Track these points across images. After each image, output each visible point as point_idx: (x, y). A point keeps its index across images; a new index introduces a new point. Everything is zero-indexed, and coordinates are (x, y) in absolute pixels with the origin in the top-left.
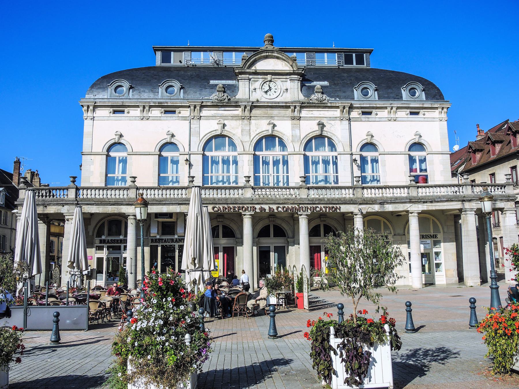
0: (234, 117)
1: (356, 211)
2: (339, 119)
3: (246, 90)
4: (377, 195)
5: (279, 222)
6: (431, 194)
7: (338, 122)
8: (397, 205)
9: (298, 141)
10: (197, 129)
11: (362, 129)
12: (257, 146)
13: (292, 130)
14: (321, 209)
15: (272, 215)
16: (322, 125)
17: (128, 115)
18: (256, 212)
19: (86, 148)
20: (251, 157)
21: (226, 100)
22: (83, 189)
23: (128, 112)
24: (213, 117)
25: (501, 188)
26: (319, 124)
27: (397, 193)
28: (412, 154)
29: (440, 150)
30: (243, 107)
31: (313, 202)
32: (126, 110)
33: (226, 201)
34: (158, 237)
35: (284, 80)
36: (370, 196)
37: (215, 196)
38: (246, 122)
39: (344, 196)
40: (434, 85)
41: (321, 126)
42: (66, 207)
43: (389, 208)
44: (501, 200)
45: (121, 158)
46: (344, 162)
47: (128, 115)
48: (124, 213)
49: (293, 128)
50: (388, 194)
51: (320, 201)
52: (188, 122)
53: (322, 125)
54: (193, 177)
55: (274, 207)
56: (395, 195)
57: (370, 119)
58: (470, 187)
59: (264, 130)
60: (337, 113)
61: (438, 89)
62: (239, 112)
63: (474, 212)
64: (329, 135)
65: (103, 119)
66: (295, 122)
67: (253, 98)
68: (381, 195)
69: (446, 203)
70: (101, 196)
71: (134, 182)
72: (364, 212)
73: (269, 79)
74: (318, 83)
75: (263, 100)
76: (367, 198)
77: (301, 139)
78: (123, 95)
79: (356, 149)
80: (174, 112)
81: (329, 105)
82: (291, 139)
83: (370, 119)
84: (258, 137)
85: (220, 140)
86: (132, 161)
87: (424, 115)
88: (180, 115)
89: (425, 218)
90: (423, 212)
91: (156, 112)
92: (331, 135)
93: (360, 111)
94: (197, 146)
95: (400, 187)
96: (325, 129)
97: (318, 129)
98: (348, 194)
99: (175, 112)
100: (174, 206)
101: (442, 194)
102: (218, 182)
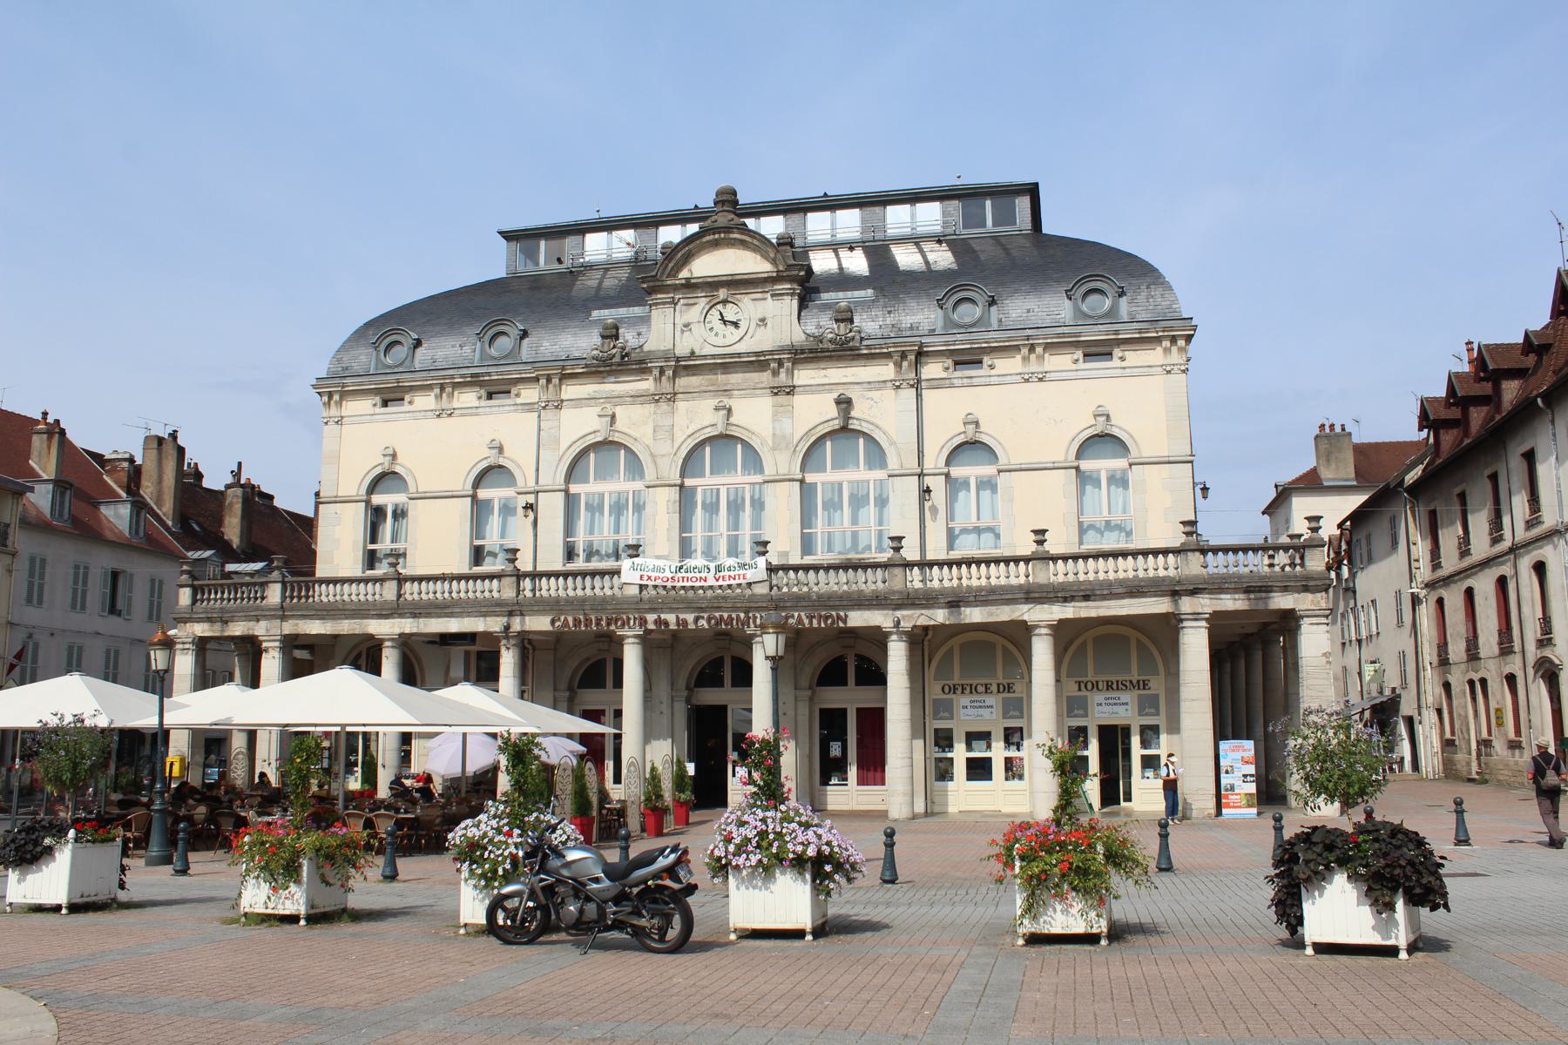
0: (637, 397)
3: (667, 328)
4: (946, 584)
6: (1091, 576)
8: (993, 609)
9: (787, 447)
11: (951, 406)
12: (691, 462)
13: (774, 421)
14: (800, 620)
16: (844, 403)
18: (648, 632)
21: (617, 359)
23: (411, 403)
26: (838, 402)
27: (998, 576)
28: (1086, 465)
29: (1163, 451)
30: (656, 372)
37: (561, 593)
38: (664, 406)
42: (263, 623)
43: (974, 615)
44: (1285, 589)
49: (775, 414)
51: (799, 601)
53: (844, 403)
55: (690, 617)
56: (993, 581)
60: (887, 371)
62: (647, 385)
64: (865, 428)
66: (782, 399)
67: (682, 350)
68: (955, 582)
69: (1126, 601)
70: (331, 598)
72: (906, 625)
74: (841, 295)
79: (935, 459)
84: (691, 443)
85: (605, 454)
86: (417, 510)
87: (1122, 359)
88: (519, 401)
91: (468, 398)
94: (553, 475)
96: (853, 414)
101: (1121, 575)
102: (591, 554)
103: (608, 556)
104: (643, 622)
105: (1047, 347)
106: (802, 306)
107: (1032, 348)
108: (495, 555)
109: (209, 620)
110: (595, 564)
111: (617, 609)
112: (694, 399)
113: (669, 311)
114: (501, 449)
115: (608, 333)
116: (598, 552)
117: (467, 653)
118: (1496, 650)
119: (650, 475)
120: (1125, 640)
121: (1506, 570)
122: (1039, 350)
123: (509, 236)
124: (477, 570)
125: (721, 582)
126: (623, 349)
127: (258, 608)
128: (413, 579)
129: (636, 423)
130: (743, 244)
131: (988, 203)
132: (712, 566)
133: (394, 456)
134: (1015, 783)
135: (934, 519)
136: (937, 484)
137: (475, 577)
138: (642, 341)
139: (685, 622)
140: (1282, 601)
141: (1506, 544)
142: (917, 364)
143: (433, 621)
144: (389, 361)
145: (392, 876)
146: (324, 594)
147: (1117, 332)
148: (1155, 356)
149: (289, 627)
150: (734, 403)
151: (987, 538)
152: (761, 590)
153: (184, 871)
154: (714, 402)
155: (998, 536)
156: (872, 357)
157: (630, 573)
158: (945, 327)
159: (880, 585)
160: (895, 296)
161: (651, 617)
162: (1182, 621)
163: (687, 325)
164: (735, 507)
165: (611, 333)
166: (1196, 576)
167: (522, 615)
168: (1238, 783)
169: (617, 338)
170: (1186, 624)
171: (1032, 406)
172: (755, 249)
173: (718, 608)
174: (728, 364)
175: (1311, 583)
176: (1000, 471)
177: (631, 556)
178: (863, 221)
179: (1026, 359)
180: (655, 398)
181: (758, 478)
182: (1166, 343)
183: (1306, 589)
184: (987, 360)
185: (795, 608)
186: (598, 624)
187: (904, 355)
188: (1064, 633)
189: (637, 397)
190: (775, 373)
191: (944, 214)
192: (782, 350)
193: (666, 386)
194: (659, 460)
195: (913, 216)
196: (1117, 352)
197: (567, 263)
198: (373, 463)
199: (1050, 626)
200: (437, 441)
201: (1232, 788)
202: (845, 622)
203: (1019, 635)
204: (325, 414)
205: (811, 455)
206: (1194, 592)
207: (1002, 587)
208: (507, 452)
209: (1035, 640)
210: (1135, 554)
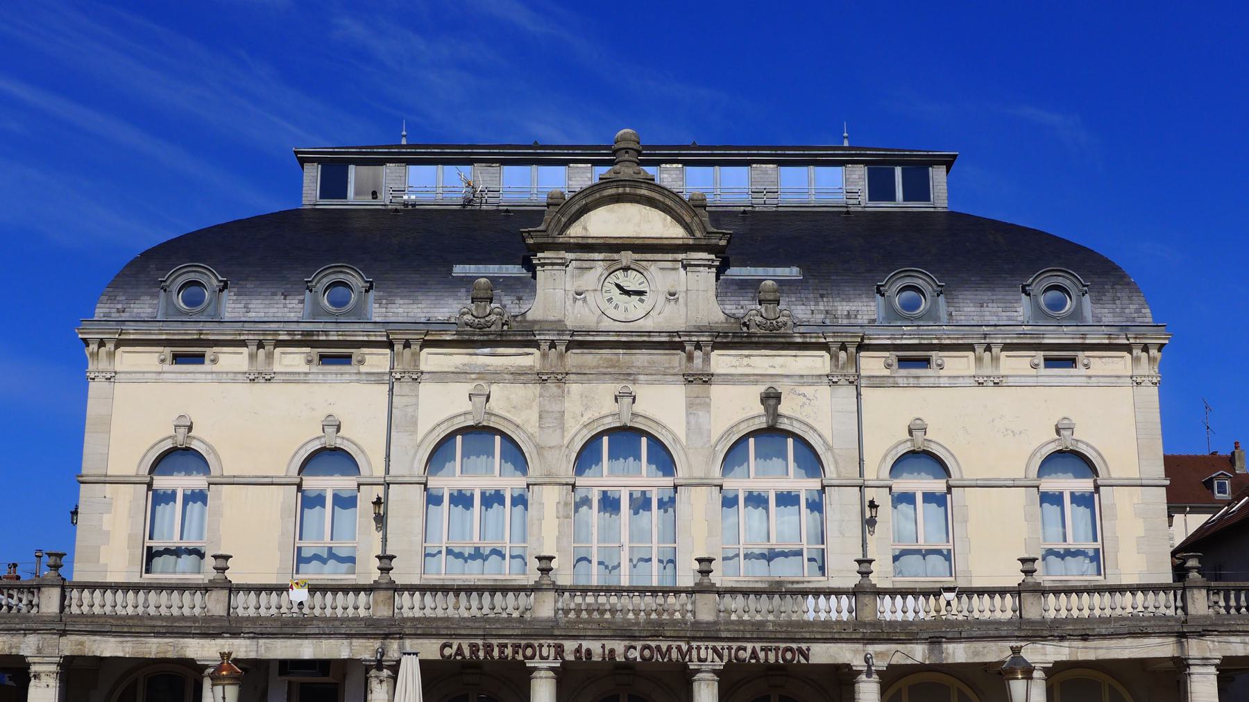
0: (518, 375)
1: (858, 663)
2: (826, 380)
4: (922, 615)
7: (824, 390)
8: (979, 646)
10: (410, 410)
11: (894, 410)
12: (587, 456)
13: (688, 415)
16: (771, 399)
17: (215, 368)
18: (565, 663)
19: (89, 466)
22: (82, 587)
24: (459, 375)
27: (983, 608)
28: (1051, 484)
29: (1133, 473)
30: (545, 346)
32: (209, 352)
35: (669, 265)
36: (899, 616)
37: (451, 612)
38: (552, 388)
41: (772, 402)
43: (958, 653)
45: (189, 492)
46: (843, 509)
47: (215, 368)
49: (690, 406)
50: (958, 609)
52: (387, 387)
53: (771, 399)
54: (392, 558)
55: (619, 646)
57: (923, 382)
58: (1204, 592)
59: (604, 412)
62: (529, 359)
63: (1213, 670)
64: (797, 429)
66: (697, 388)
69: (1128, 642)
72: (881, 664)
75: (606, 324)
76: (891, 624)
77: (714, 440)
78: (203, 311)
79: (877, 467)
80: (346, 359)
81: (799, 340)
83: (923, 382)
84: (586, 435)
87: (1087, 366)
88: (363, 369)
91: (293, 360)
92: (804, 428)
93: (892, 356)
94: (410, 462)
96: (782, 409)
98: (839, 610)
99: (349, 357)
100: (333, 641)
104: (560, 650)
105: (1007, 347)
107: (988, 348)
112: (589, 382)
113: (557, 272)
117: (290, 683)
122: (996, 350)
124: (148, 578)
127: (26, 618)
128: (248, 589)
129: (515, 406)
136: (882, 498)
137: (148, 588)
139: (612, 651)
146: (82, 603)
147: (1084, 336)
149: (69, 646)
150: (641, 391)
158: (887, 318)
161: (570, 646)
162: (1188, 666)
166: (1201, 617)
173: (655, 636)
176: (949, 488)
179: (979, 360)
180: (541, 378)
186: (502, 652)
189: (518, 375)
190: (690, 358)
192: (700, 330)
198: (156, 434)
199: (1045, 670)
202: (807, 658)
206: (1201, 634)
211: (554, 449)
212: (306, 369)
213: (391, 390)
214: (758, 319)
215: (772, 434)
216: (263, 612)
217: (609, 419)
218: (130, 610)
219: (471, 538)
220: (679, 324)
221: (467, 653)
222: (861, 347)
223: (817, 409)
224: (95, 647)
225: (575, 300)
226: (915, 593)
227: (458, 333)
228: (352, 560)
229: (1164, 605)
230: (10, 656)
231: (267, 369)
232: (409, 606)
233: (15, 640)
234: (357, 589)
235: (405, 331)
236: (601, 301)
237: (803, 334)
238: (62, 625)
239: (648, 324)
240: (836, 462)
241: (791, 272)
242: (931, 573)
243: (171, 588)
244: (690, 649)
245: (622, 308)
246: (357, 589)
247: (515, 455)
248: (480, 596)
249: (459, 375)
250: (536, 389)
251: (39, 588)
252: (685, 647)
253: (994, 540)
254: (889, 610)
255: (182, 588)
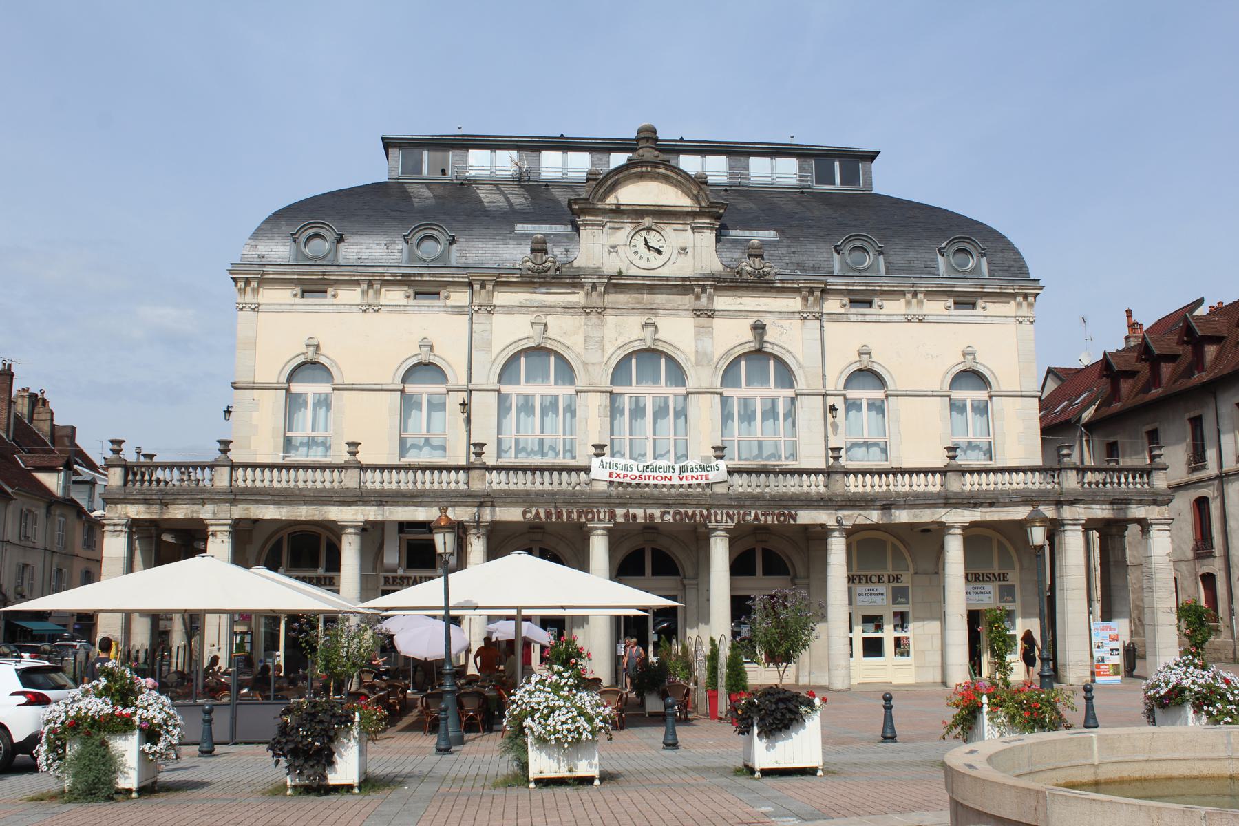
0: (568, 309)
2: (797, 315)
3: (598, 248)
4: (877, 489)
5: (664, 544)
6: (992, 487)
7: (797, 323)
8: (917, 511)
12: (620, 372)
13: (696, 340)
15: (650, 528)
16: (759, 328)
17: (335, 301)
18: (616, 524)
20: (605, 399)
24: (524, 308)
25: (1141, 476)
27: (920, 484)
28: (957, 395)
29: (1016, 387)
30: (588, 287)
31: (742, 502)
33: (549, 498)
34: (400, 572)
35: (680, 227)
36: (860, 489)
37: (529, 487)
39: (805, 489)
40: (1009, 243)
43: (902, 516)
44: (1140, 502)
46: (810, 410)
47: (335, 301)
48: (334, 522)
49: (697, 334)
50: (902, 485)
52: (467, 317)
53: (759, 328)
55: (657, 513)
56: (915, 488)
59: (636, 337)
60: (794, 303)
61: (1017, 253)
62: (578, 298)
63: (1080, 528)
64: (777, 351)
65: (278, 307)
66: (703, 321)
68: (884, 488)
71: (353, 454)
72: (848, 524)
73: (647, 225)
74: (755, 233)
75: (634, 271)
77: (715, 360)
79: (835, 382)
82: (693, 359)
87: (984, 309)
88: (449, 303)
89: (975, 536)
90: (974, 525)
91: (395, 296)
94: (486, 374)
95: (926, 472)
96: (766, 338)
97: (751, 338)
98: (814, 486)
101: (1015, 486)
103: (535, 453)
104: (613, 516)
105: (928, 294)
106: (718, 241)
107: (915, 294)
108: (420, 448)
109: (147, 502)
110: (524, 460)
111: (587, 502)
113: (597, 232)
114: (431, 347)
115: (539, 247)
116: (524, 449)
118: (1190, 555)
119: (581, 381)
120: (883, 543)
121: (1209, 492)
122: (920, 296)
123: (389, 144)
125: (684, 482)
126: (554, 262)
128: (374, 468)
129: (567, 332)
130: (666, 179)
131: (837, 164)
132: (677, 467)
133: (318, 347)
134: (900, 659)
135: (835, 434)
136: (839, 403)
138: (572, 257)
139: (652, 516)
140: (1137, 512)
141: (1212, 469)
142: (820, 301)
143: (400, 509)
144: (307, 251)
145: (672, 744)
147: (983, 287)
148: (1008, 308)
149: (238, 512)
151: (875, 451)
152: (720, 489)
153: (672, 744)
154: (643, 319)
155: (885, 451)
156: (783, 290)
157: (600, 472)
158: (841, 270)
159: (822, 489)
160: (796, 239)
161: (620, 512)
162: (1063, 525)
163: (613, 247)
164: (661, 412)
165: (539, 248)
167: (493, 505)
168: (1107, 656)
169: (546, 253)
170: (1067, 528)
171: (916, 340)
172: (677, 185)
173: (684, 505)
174: (655, 286)
175: (1160, 498)
176: (887, 396)
177: (597, 455)
178: (731, 167)
179: (908, 303)
180: (585, 311)
181: (681, 390)
182: (1019, 299)
183: (1155, 503)
184: (877, 301)
185: (752, 506)
187: (811, 291)
188: (854, 535)
189: (568, 309)
190: (698, 297)
191: (801, 169)
192: (705, 277)
193: (595, 300)
194: (591, 368)
195: (773, 168)
196: (980, 303)
197: (451, 174)
198: (293, 350)
199: (964, 528)
200: (371, 335)
201: (1103, 660)
202: (795, 520)
203: (934, 535)
204: (239, 300)
205: (730, 374)
206: (1072, 503)
207: (924, 493)
208: (436, 351)
209: (712, 540)
210: (995, 471)
211: (595, 366)
212: (405, 302)
213: (471, 319)
214: (749, 269)
215: (758, 357)
216: (386, 486)
217: (637, 343)
218: (284, 485)
219: (533, 431)
220: (688, 273)
221: (543, 516)
222: (824, 291)
223: (792, 336)
224: (258, 512)
225: (610, 252)
226: (872, 472)
227: (522, 276)
228: (443, 448)
229: (1035, 482)
230: (192, 520)
231: (376, 302)
232: (497, 482)
233: (196, 507)
234: (449, 469)
235: (481, 275)
236: (629, 252)
237: (782, 281)
238: (234, 496)
239: (664, 272)
240: (806, 377)
241: (771, 234)
242: (873, 460)
243: (306, 467)
244: (709, 515)
245: (645, 259)
246: (449, 469)
247: (566, 371)
248: (551, 474)
249: (524, 308)
250: (581, 320)
251: (1060, 470)
252: (705, 512)
253: (918, 437)
254: (855, 485)
255: (314, 467)
